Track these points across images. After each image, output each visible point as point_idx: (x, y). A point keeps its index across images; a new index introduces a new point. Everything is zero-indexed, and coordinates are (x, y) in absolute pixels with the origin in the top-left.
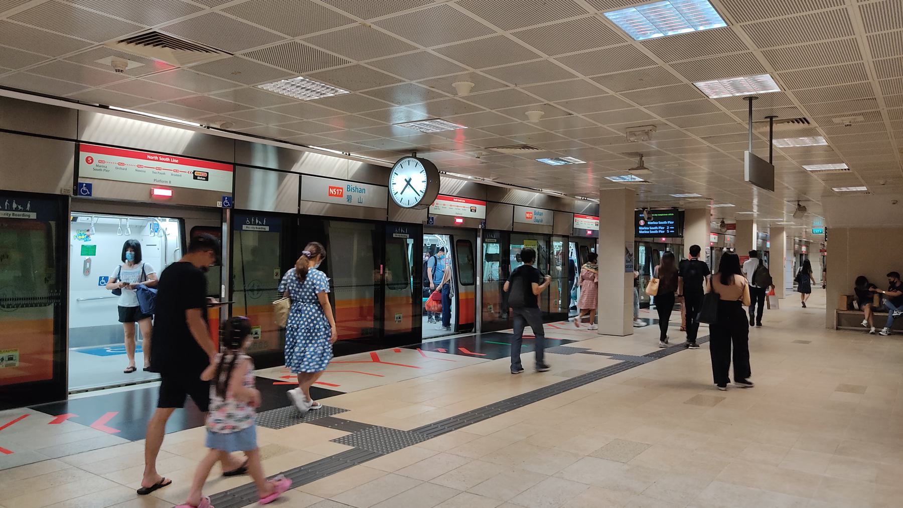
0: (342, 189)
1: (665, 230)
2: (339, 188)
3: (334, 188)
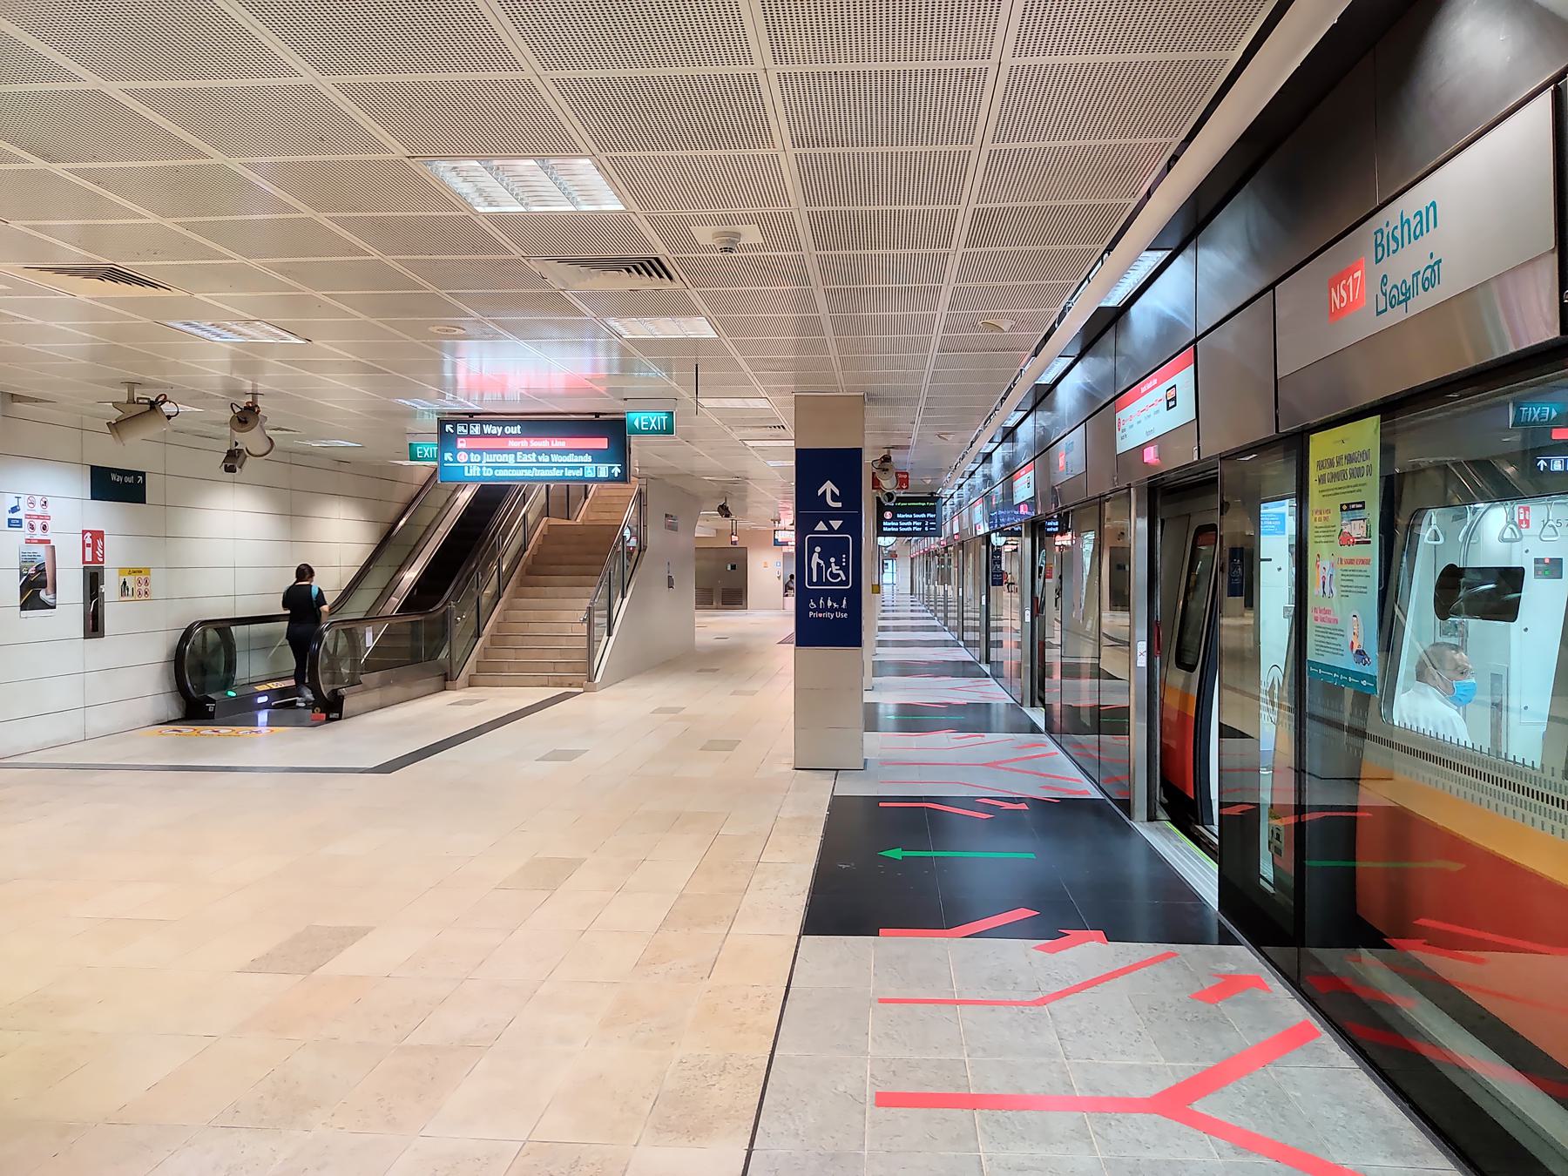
1: (923, 526)
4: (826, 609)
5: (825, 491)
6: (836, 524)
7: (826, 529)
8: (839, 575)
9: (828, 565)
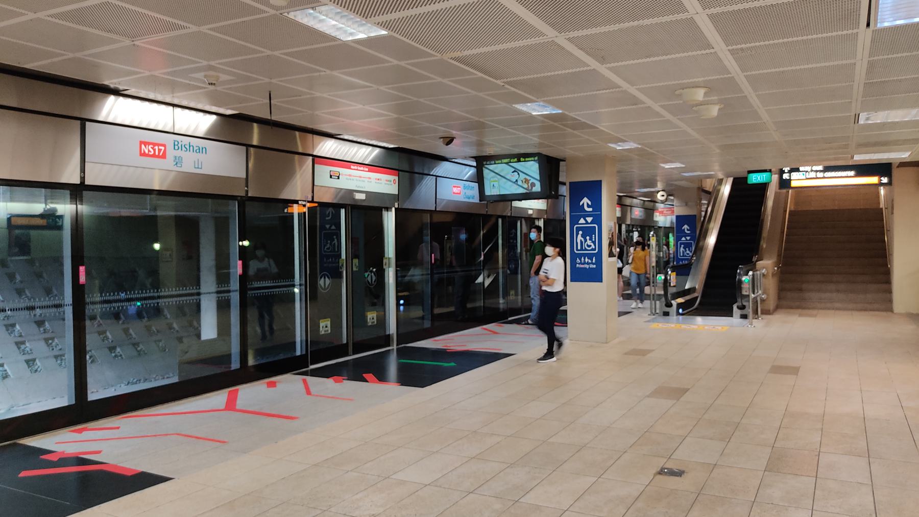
0: (164, 145)
2: (159, 145)
3: (149, 144)
4: (585, 263)
5: (583, 204)
6: (589, 219)
7: (584, 222)
8: (591, 246)
9: (586, 241)
